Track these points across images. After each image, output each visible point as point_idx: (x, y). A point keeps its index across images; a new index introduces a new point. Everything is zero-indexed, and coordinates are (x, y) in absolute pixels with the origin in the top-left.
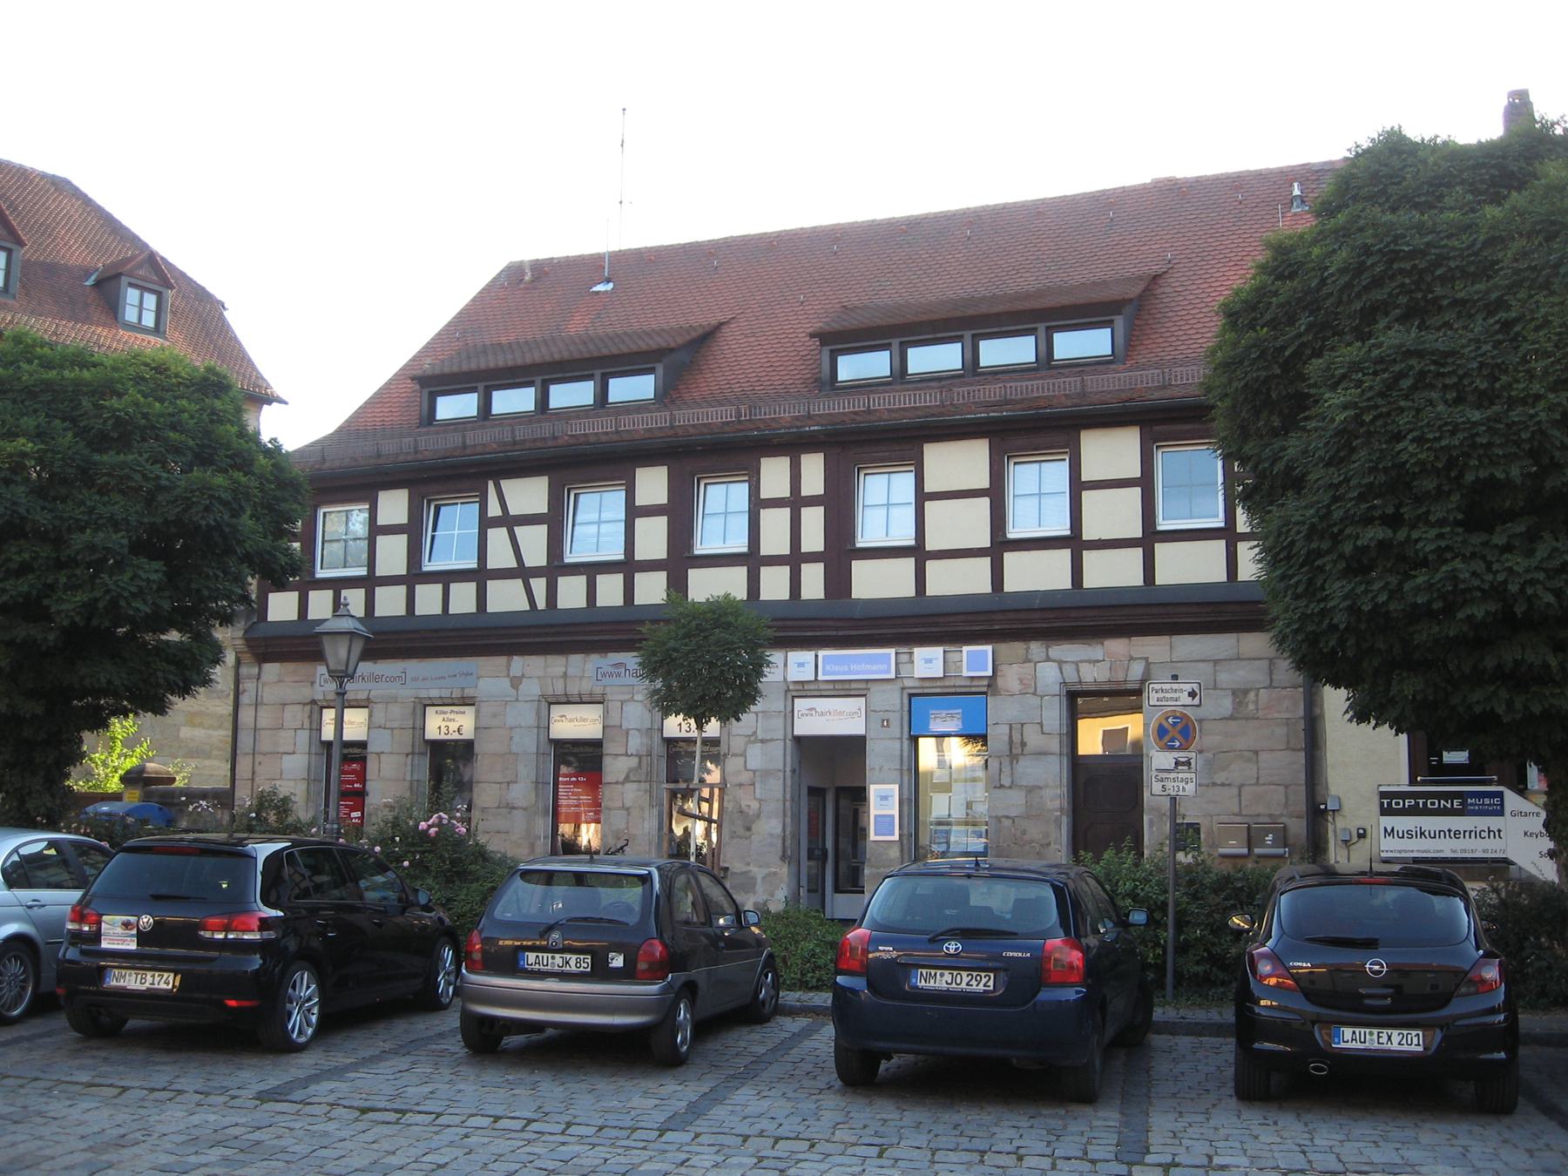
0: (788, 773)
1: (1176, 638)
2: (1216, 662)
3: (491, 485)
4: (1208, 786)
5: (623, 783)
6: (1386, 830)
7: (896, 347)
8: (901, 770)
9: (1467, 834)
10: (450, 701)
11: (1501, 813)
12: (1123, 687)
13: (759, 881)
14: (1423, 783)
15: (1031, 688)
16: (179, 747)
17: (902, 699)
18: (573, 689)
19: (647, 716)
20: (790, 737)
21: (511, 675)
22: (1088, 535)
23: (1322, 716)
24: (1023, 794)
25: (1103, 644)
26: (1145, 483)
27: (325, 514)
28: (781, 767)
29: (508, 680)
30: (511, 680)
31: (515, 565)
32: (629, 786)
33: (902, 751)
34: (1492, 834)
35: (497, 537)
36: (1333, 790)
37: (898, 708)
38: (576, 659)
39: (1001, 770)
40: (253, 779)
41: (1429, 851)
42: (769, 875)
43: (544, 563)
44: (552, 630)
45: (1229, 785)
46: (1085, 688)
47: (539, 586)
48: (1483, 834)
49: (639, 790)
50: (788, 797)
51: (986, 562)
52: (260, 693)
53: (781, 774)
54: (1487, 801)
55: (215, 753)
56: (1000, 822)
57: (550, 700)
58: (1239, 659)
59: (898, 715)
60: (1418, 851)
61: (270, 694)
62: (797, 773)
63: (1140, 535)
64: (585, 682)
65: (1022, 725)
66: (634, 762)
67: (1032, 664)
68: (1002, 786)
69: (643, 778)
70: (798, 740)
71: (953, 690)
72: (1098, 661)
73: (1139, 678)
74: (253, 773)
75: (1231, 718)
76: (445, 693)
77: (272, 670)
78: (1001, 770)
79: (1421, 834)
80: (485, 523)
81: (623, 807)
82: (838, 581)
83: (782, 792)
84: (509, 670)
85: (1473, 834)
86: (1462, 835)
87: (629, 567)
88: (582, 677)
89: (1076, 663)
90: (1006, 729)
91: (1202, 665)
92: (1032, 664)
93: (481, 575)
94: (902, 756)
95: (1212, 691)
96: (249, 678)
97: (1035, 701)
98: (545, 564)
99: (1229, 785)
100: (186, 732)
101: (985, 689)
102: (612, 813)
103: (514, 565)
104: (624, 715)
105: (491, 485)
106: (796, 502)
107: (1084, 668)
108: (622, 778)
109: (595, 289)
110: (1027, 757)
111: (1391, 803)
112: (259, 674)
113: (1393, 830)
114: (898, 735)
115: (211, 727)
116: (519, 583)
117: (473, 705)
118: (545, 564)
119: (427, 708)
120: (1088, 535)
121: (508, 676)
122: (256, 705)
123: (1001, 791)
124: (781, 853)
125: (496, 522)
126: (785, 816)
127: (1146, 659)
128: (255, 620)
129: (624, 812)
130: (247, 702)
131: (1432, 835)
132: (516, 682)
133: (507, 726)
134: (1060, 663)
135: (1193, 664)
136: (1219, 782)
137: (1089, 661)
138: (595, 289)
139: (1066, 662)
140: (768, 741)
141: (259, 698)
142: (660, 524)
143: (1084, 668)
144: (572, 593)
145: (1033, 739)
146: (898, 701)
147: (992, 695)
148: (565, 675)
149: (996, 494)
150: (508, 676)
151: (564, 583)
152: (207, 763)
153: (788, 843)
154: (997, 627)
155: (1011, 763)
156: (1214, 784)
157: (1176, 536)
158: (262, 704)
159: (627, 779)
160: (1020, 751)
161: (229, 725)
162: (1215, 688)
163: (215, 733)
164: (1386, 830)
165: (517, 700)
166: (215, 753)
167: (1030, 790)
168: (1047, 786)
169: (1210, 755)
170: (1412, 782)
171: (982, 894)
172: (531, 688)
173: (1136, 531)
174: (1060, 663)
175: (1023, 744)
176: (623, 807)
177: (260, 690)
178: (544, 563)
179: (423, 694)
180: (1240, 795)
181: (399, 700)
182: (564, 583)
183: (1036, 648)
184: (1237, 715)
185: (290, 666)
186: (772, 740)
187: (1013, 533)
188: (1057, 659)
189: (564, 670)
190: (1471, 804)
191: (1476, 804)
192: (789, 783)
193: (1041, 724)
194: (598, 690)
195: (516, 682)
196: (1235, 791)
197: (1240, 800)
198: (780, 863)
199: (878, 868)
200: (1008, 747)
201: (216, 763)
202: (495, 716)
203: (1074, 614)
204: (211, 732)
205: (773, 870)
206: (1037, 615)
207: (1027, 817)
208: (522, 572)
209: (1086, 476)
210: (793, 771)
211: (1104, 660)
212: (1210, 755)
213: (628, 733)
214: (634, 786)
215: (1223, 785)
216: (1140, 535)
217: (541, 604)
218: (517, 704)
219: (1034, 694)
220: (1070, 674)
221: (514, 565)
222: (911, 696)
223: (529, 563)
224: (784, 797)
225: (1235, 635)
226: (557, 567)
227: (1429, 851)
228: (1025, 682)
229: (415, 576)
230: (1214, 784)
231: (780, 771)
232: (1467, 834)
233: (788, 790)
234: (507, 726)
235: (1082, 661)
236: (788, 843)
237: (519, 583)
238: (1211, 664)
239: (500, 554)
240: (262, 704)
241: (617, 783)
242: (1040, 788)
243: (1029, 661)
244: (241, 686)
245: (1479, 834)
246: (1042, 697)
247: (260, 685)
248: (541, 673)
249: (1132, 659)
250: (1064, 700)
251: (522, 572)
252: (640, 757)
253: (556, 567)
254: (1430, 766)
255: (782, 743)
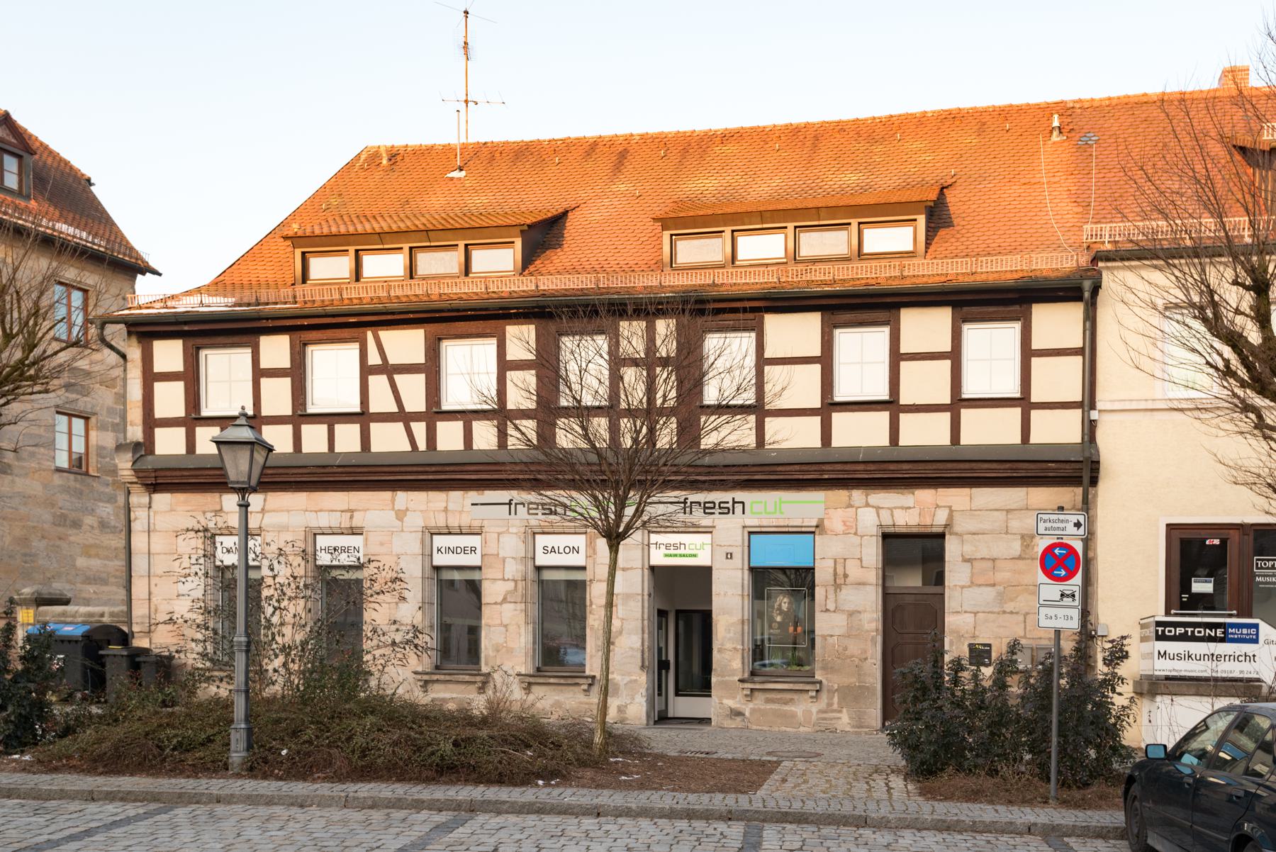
0: (646, 597)
1: (975, 490)
2: (1008, 511)
3: (370, 335)
4: (999, 613)
5: (501, 604)
6: (1159, 653)
7: (727, 235)
8: (743, 595)
9: (1227, 658)
10: (340, 531)
11: (1256, 641)
12: (929, 530)
13: (622, 687)
14: (1176, 615)
15: (852, 529)
16: (77, 575)
17: (743, 536)
18: (454, 522)
19: (522, 546)
20: (647, 566)
21: (396, 508)
22: (904, 400)
23: (1095, 558)
24: (845, 617)
25: (913, 494)
26: (955, 356)
27: (206, 355)
28: (640, 592)
29: (393, 513)
30: (396, 514)
31: (396, 410)
32: (506, 606)
33: (743, 579)
34: (1248, 658)
35: (378, 384)
36: (1102, 619)
37: (740, 543)
38: (456, 495)
39: (827, 597)
40: (149, 599)
41: (1195, 671)
42: (631, 682)
43: (423, 409)
44: (433, 469)
45: (1017, 613)
46: (897, 530)
47: (419, 429)
48: (1240, 658)
49: (516, 610)
50: (646, 616)
51: (817, 420)
52: (152, 521)
53: (640, 598)
54: (1245, 631)
55: (112, 580)
56: (826, 639)
57: (432, 531)
58: (1027, 509)
59: (740, 549)
60: (1185, 671)
61: (161, 522)
62: (652, 597)
63: (819, 406)
64: (464, 515)
65: (845, 559)
66: (511, 585)
67: (854, 509)
68: (827, 610)
69: (519, 600)
70: (653, 569)
71: (786, 530)
72: (910, 508)
73: (944, 523)
74: (150, 594)
75: (1020, 558)
76: (335, 524)
77: (162, 500)
78: (827, 597)
79: (1189, 656)
80: (366, 371)
81: (501, 624)
82: (689, 433)
83: (640, 613)
84: (393, 504)
85: (1232, 658)
86: (1223, 659)
87: (501, 414)
88: (461, 512)
89: (891, 509)
90: (831, 563)
91: (996, 513)
92: (854, 509)
93: (363, 417)
94: (743, 583)
95: (1004, 535)
96: (140, 507)
97: (856, 540)
98: (424, 410)
99: (1017, 613)
100: (81, 562)
101: (813, 529)
102: (492, 629)
103: (396, 410)
104: (501, 545)
105: (370, 335)
106: (650, 362)
107: (897, 513)
108: (500, 599)
109: (449, 175)
110: (849, 587)
111: (1163, 632)
112: (150, 503)
113: (1165, 653)
114: (740, 567)
115: (107, 558)
116: (400, 426)
117: (362, 534)
118: (424, 410)
119: (318, 537)
120: (904, 400)
121: (393, 509)
122: (149, 532)
123: (827, 614)
124: (640, 664)
125: (376, 370)
126: (643, 633)
127: (950, 507)
128: (143, 453)
129: (503, 629)
130: (140, 529)
131: (1198, 658)
132: (401, 515)
133: (394, 553)
134: (878, 508)
135: (989, 512)
136: (1008, 610)
137: (902, 508)
138: (449, 175)
139: (883, 508)
140: (628, 569)
141: (152, 526)
142: (530, 378)
143: (897, 513)
144: (450, 437)
145: (854, 571)
146: (740, 538)
147: (820, 534)
148: (446, 510)
149: (826, 360)
150: (393, 509)
151: (442, 427)
152: (105, 588)
153: (646, 655)
154: (826, 477)
155: (836, 592)
156: (1004, 612)
157: (978, 403)
158: (155, 531)
159: (505, 600)
160: (842, 581)
161: (123, 556)
162: (1007, 533)
163: (111, 563)
164: (1159, 653)
165: (402, 531)
166: (112, 580)
167: (851, 614)
168: (865, 611)
169: (1001, 588)
170: (1167, 613)
171: (812, 697)
172: (416, 521)
173: (946, 399)
174: (878, 508)
175: (846, 576)
176: (501, 624)
177: (152, 518)
178: (423, 409)
179: (314, 524)
180: (1025, 622)
181: (290, 529)
182: (442, 427)
183: (857, 495)
184: (1023, 556)
185: (181, 497)
186: (631, 568)
187: (839, 397)
188: (874, 505)
189: (444, 505)
190: (1232, 634)
191: (1235, 634)
192: (646, 604)
193: (861, 559)
194: (476, 524)
195: (401, 515)
196: (1021, 618)
197: (1025, 626)
198: (640, 672)
199: (723, 676)
200: (833, 578)
201: (114, 588)
202: (382, 544)
203: (892, 467)
204: (107, 562)
205: (634, 678)
206: (861, 467)
207: (848, 636)
208: (403, 416)
209: (904, 349)
210: (650, 595)
211: (914, 507)
212: (1001, 588)
213: (504, 561)
214: (512, 606)
215: (1012, 613)
216: (819, 406)
217: (422, 445)
218: (403, 534)
219: (856, 534)
220: (887, 520)
221: (396, 410)
222: (750, 533)
223: (408, 408)
224: (643, 617)
225: (1025, 489)
226: (301, 415)
227: (1195, 671)
228: (848, 524)
229: (300, 417)
230: (1004, 612)
231: (638, 594)
232: (1227, 658)
233: (646, 611)
234: (394, 553)
235: (895, 508)
236: (646, 655)
237: (400, 426)
238: (1005, 513)
239: (381, 400)
240: (155, 531)
241: (496, 603)
242: (859, 612)
243: (852, 506)
244: (132, 514)
245: (1236, 658)
246: (862, 537)
247: (152, 514)
248: (423, 507)
249: (938, 506)
250: (880, 539)
251: (403, 416)
252: (516, 581)
253: (829, 407)
254: (1182, 602)
255: (640, 571)
